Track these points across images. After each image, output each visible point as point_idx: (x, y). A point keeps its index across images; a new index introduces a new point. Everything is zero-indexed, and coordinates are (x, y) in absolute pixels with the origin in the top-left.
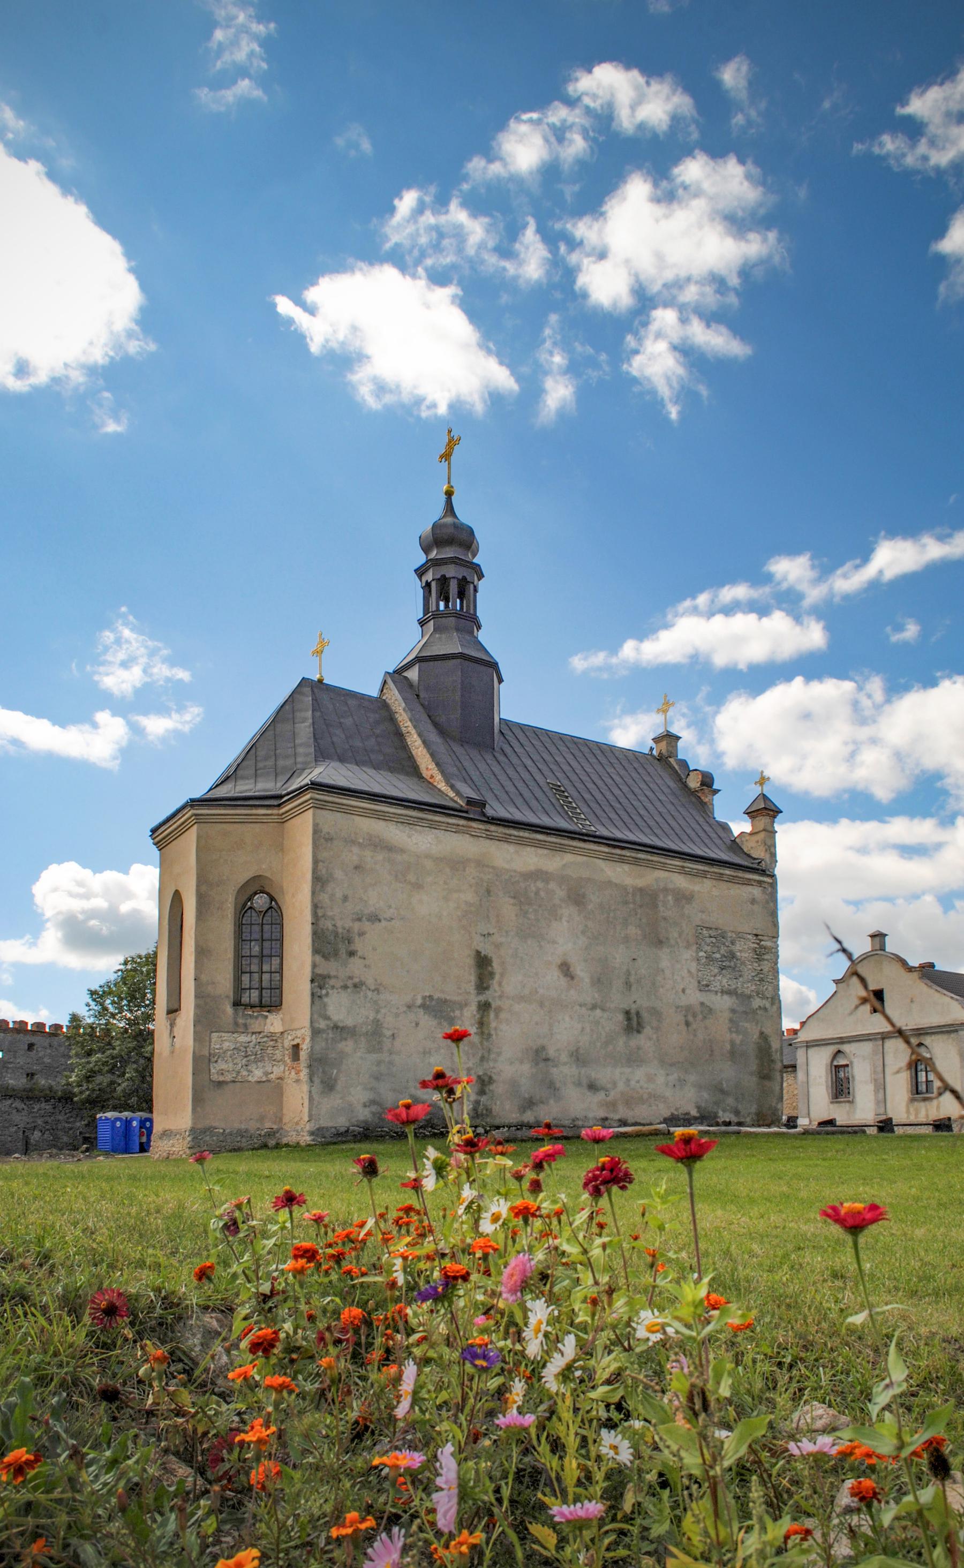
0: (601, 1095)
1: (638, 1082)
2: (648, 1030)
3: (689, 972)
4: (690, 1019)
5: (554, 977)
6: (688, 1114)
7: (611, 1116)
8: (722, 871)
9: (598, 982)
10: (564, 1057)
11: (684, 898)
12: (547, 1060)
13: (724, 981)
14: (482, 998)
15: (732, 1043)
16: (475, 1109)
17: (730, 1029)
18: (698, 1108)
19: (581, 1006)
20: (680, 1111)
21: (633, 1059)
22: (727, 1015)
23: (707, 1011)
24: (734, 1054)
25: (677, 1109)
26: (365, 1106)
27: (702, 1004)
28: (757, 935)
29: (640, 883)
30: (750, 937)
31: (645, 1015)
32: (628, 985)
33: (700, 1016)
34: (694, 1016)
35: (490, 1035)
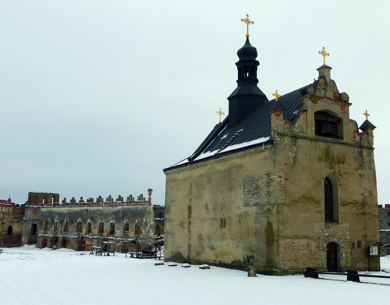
0: (214, 251)
1: (224, 246)
2: (227, 226)
3: (241, 199)
4: (241, 219)
5: (204, 210)
6: (240, 260)
7: (217, 260)
8: (250, 151)
9: (214, 209)
10: (206, 238)
11: (239, 167)
12: (202, 239)
13: (254, 201)
14: (189, 220)
15: (256, 227)
16: (188, 255)
17: (255, 222)
18: (243, 258)
19: (210, 219)
20: (237, 259)
21: (223, 238)
22: (254, 215)
23: (247, 214)
24: (256, 234)
25: (236, 258)
26: (171, 253)
27: (245, 212)
28: (267, 174)
29: (226, 168)
30: (265, 176)
31: (227, 220)
32: (222, 209)
33: (244, 218)
34: (242, 218)
35: (191, 231)
